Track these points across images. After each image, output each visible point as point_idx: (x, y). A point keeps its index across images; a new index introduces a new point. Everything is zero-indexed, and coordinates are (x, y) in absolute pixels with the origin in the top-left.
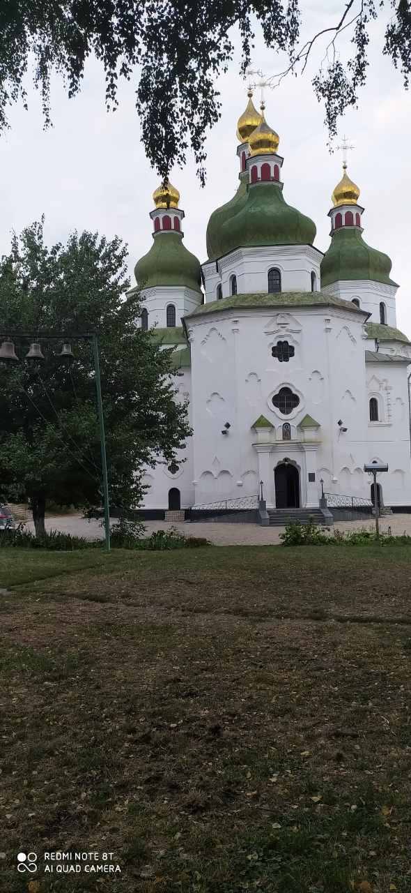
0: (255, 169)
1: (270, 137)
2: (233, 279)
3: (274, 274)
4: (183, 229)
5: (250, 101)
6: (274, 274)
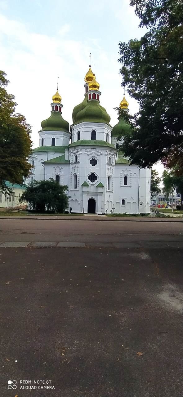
1: (97, 85)
2: (79, 133)
3: (94, 133)
6: (94, 133)
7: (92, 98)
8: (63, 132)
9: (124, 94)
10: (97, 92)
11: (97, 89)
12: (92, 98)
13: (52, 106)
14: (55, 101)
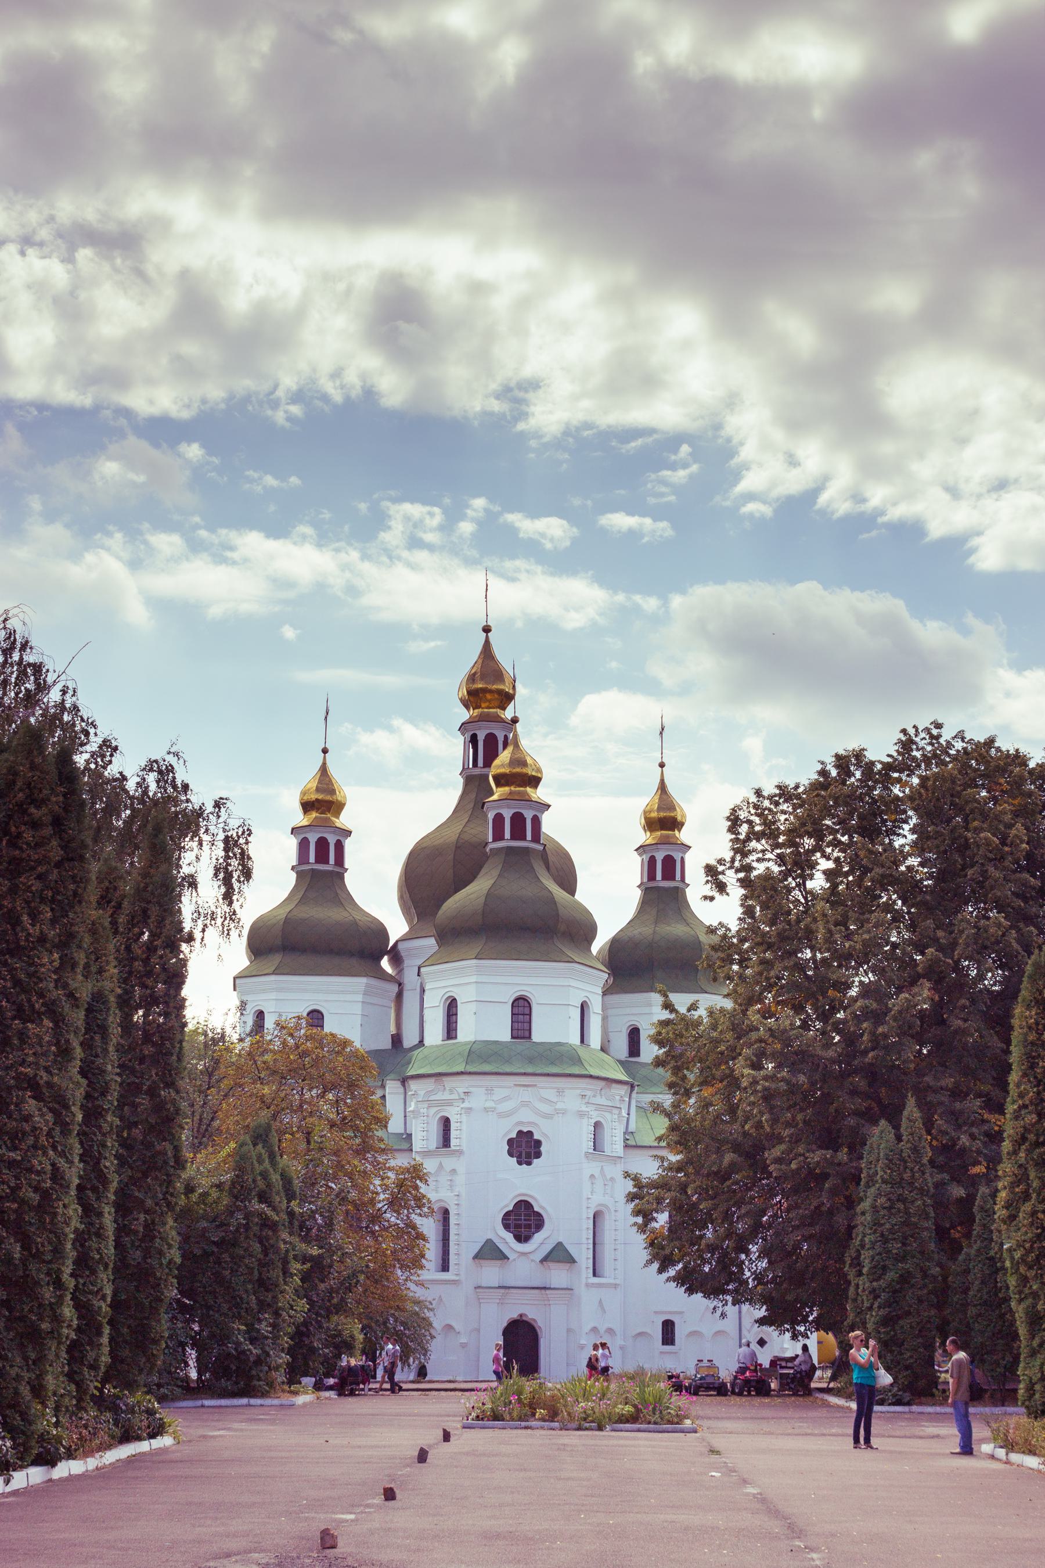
0: (499, 819)
1: (530, 772)
2: (451, 1008)
3: (522, 1010)
4: (347, 864)
5: (487, 637)
6: (522, 1010)
8: (363, 981)
10: (531, 808)
12: (507, 835)
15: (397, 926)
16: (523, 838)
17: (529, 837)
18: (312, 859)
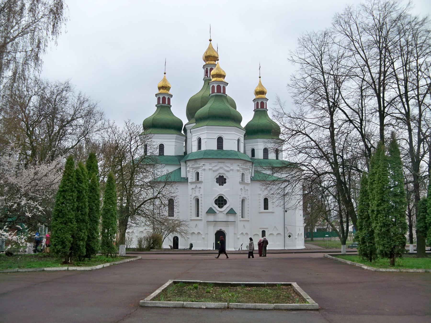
0: (213, 87)
1: (223, 73)
2: (200, 140)
3: (220, 140)
5: (210, 43)
6: (220, 140)
7: (216, 91)
8: (176, 135)
9: (260, 77)
11: (221, 79)
12: (216, 91)
13: (158, 97)
14: (162, 91)
15: (185, 121)
16: (221, 92)
17: (222, 92)
18: (161, 103)
